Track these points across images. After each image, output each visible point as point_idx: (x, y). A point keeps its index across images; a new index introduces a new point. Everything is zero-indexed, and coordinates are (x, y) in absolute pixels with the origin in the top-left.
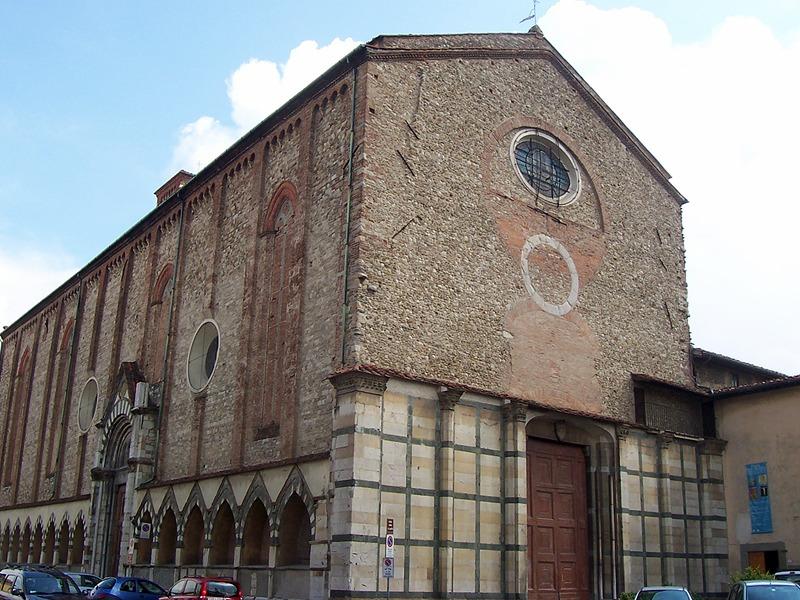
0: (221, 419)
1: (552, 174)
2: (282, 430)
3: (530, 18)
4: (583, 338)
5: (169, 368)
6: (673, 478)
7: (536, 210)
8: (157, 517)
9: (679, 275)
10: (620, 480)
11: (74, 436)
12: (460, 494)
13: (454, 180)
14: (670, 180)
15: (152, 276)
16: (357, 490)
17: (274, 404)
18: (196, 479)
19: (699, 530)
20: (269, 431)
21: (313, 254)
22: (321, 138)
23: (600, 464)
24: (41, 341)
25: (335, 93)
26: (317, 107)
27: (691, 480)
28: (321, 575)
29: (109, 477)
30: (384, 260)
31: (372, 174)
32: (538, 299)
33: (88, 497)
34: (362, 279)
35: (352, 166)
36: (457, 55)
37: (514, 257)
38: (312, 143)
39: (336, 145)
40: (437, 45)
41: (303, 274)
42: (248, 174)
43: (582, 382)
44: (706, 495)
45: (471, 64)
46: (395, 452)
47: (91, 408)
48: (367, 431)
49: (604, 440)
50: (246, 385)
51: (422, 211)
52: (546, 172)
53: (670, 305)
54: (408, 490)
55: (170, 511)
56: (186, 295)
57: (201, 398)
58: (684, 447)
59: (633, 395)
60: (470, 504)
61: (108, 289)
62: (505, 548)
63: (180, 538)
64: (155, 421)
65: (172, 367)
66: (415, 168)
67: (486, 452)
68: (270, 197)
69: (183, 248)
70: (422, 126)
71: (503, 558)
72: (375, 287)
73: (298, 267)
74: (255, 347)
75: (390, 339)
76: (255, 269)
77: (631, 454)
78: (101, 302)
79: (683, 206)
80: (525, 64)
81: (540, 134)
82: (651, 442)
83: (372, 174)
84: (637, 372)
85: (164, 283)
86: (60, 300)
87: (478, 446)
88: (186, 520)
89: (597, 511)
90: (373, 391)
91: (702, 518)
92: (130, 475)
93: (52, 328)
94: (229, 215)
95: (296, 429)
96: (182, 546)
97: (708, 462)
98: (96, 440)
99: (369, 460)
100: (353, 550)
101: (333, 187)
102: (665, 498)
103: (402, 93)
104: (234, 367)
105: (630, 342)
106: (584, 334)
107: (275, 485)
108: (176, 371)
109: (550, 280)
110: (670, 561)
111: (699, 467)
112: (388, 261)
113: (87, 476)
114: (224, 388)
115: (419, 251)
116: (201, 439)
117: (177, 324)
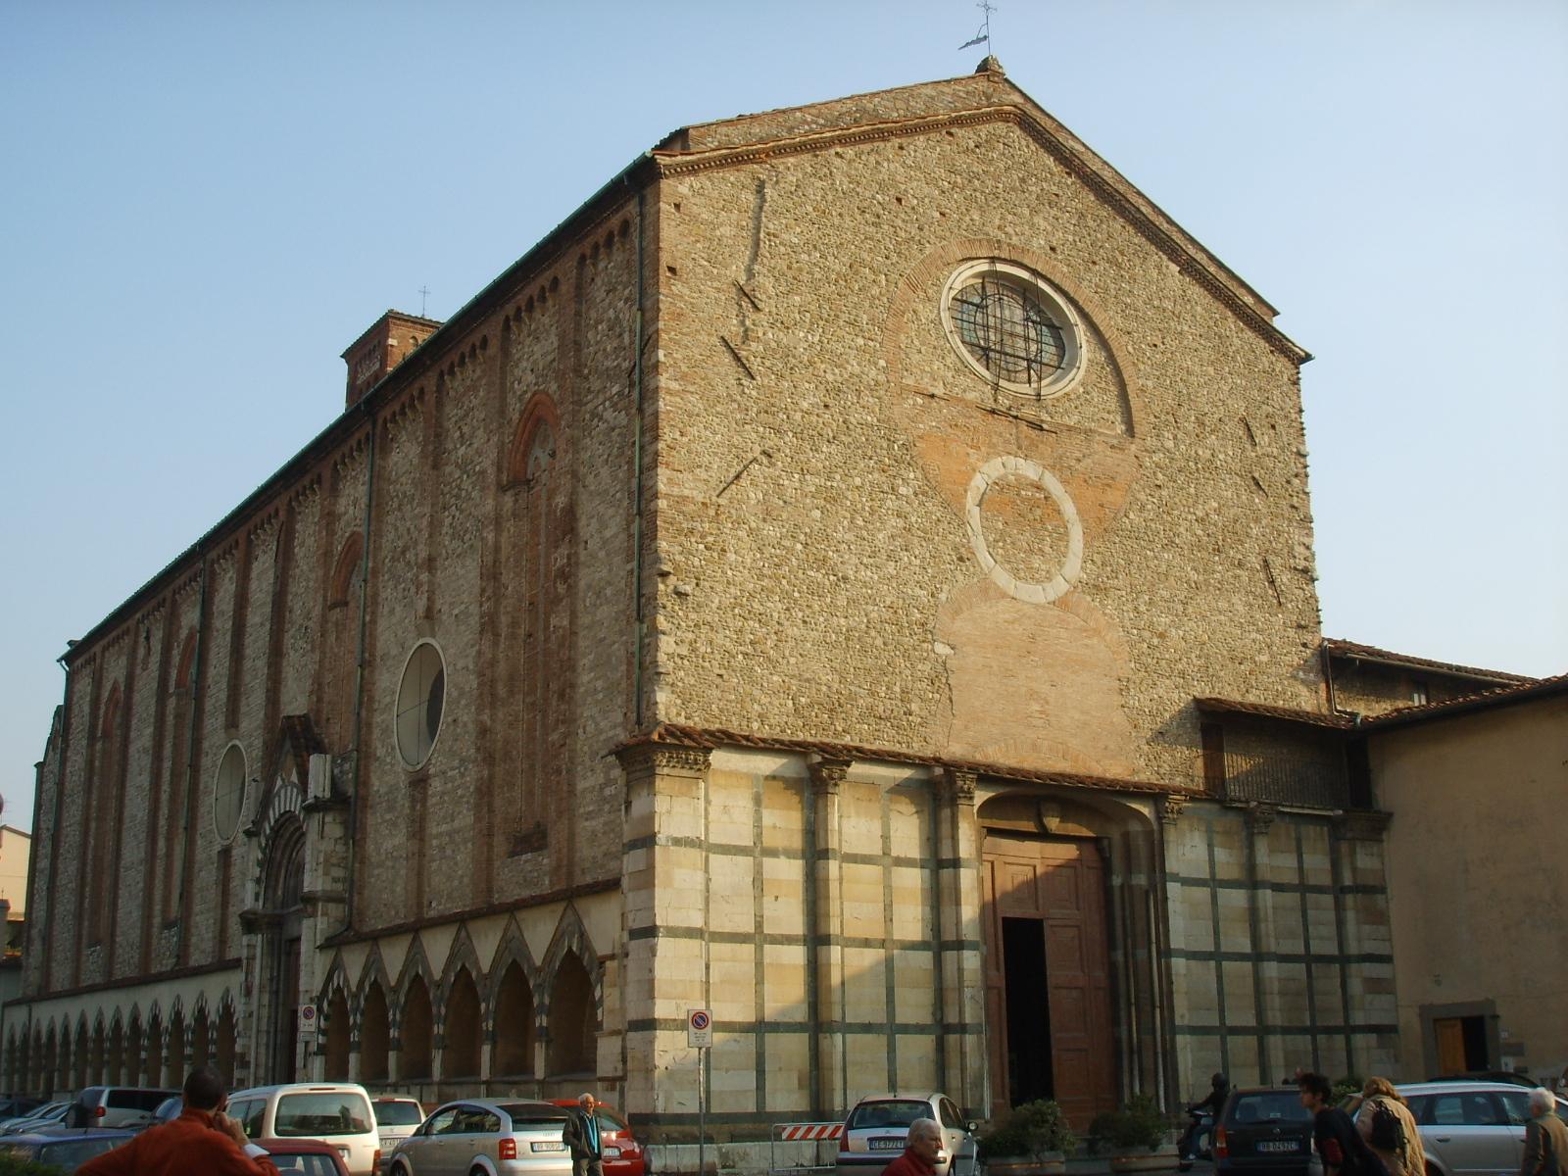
0: (453, 819)
1: (1027, 339)
2: (552, 840)
3: (978, 41)
4: (1095, 641)
5: (362, 727)
6: (1278, 888)
7: (993, 412)
8: (356, 996)
10: (1166, 899)
11: (206, 853)
12: (854, 939)
13: (830, 377)
14: (1277, 323)
15: (327, 554)
16: (663, 944)
17: (538, 791)
18: (416, 928)
20: (531, 840)
21: (587, 528)
22: (593, 315)
23: (1129, 870)
24: (138, 671)
25: (611, 235)
26: (583, 258)
27: (1320, 889)
28: (613, 1089)
29: (275, 927)
30: (703, 537)
31: (674, 386)
32: (1002, 578)
33: (235, 964)
34: (664, 575)
35: (641, 371)
36: (830, 143)
37: (953, 507)
38: (578, 324)
39: (618, 330)
40: (790, 130)
41: (573, 561)
42: (478, 372)
43: (1094, 717)
44: (1350, 916)
45: (858, 155)
46: (732, 872)
47: (235, 796)
48: (677, 842)
49: (1135, 827)
50: (489, 759)
51: (772, 441)
53: (1276, 562)
54: (758, 937)
55: (375, 985)
56: (387, 593)
57: (419, 781)
59: (1199, 735)
61: (254, 575)
62: (943, 1029)
63: (393, 1033)
64: (344, 824)
65: (369, 725)
66: (755, 365)
67: (900, 862)
68: (516, 416)
69: (376, 505)
70: (766, 284)
71: (941, 1048)
72: (688, 589)
73: (564, 550)
74: (502, 691)
75: (721, 676)
76: (497, 549)
77: (1188, 851)
78: (242, 600)
79: (1302, 367)
81: (1000, 267)
82: (1233, 821)
83: (674, 386)
84: (1207, 694)
85: (351, 565)
86: (168, 593)
87: (886, 853)
88: (402, 1000)
89: (1126, 955)
90: (685, 773)
91: (1344, 959)
92: (307, 923)
93: (157, 646)
94: (450, 446)
95: (572, 837)
96: (398, 1047)
97: (1353, 853)
98: (248, 857)
99: (678, 892)
100: (659, 1046)
101: (614, 406)
102: (1263, 926)
103: (726, 231)
104: (471, 727)
105: (1190, 637)
106: (1097, 632)
107: (539, 934)
108: (376, 733)
109: (1024, 539)
110: (1275, 1042)
112: (710, 539)
113: (234, 926)
114: (456, 763)
115: (768, 515)
116: (422, 854)
117: (373, 646)
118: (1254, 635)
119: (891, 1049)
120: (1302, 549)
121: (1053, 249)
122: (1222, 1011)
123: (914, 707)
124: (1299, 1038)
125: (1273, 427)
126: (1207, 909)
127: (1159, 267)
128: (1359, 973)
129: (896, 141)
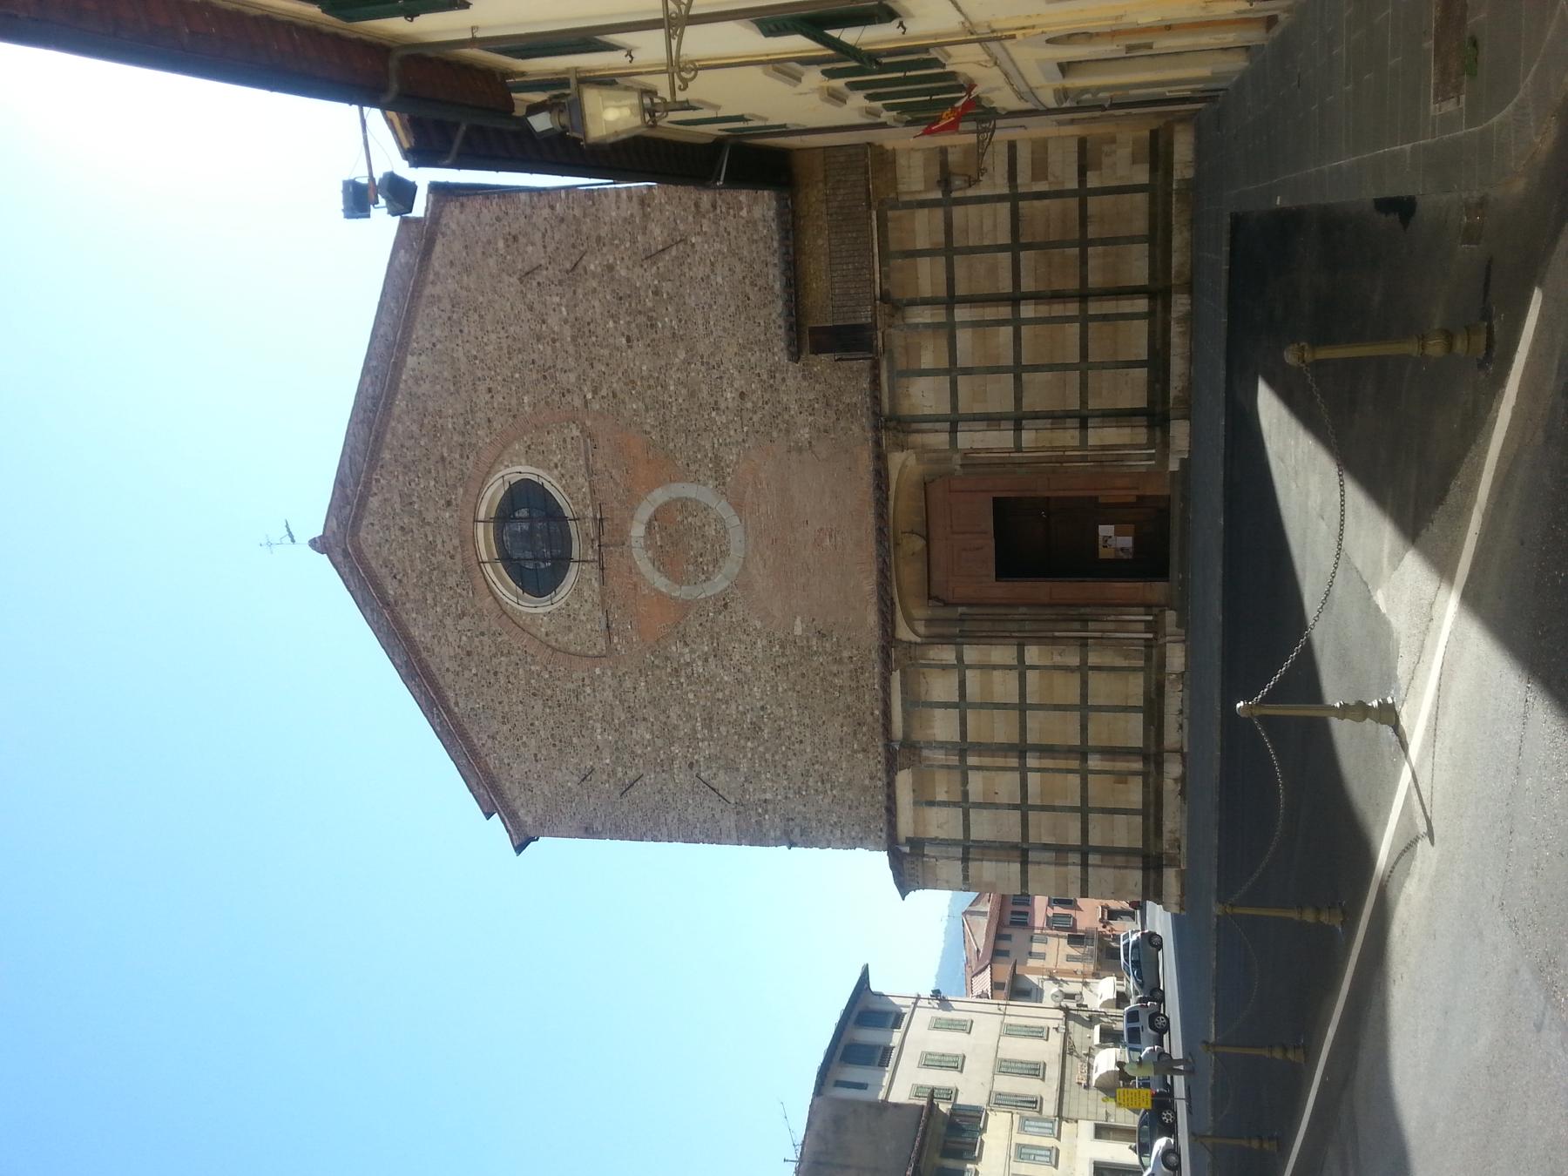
1: (530, 518)
4: (762, 475)
9: (577, 212)
19: (1036, 203)
32: (731, 567)
36: (449, 711)
44: (970, 193)
52: (531, 527)
58: (893, 247)
59: (823, 357)
60: (1034, 721)
66: (632, 774)
80: (391, 589)
81: (485, 558)
91: (1014, 198)
105: (736, 360)
111: (922, 204)
118: (719, 280)
119: (1099, 709)
120: (624, 205)
121: (449, 503)
122: (1066, 367)
123: (846, 654)
124: (1091, 263)
125: (515, 239)
126: (977, 379)
127: (417, 380)
128: (1025, 183)
129: (424, 654)
